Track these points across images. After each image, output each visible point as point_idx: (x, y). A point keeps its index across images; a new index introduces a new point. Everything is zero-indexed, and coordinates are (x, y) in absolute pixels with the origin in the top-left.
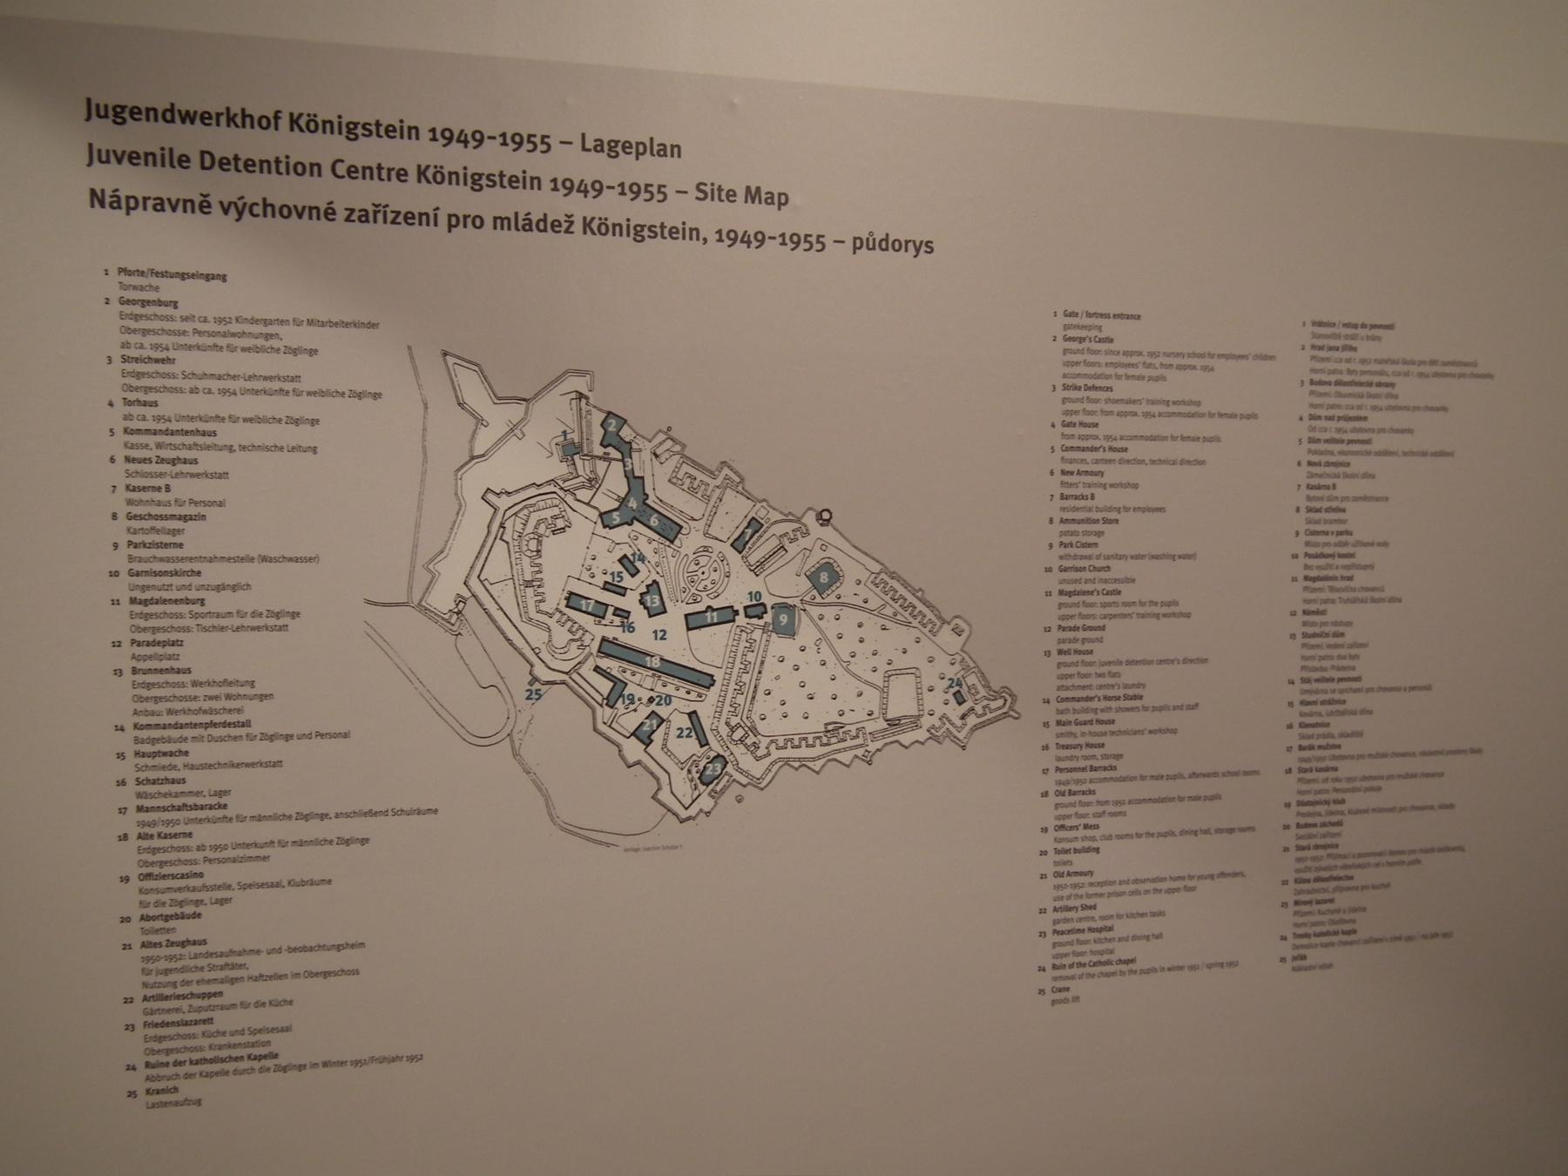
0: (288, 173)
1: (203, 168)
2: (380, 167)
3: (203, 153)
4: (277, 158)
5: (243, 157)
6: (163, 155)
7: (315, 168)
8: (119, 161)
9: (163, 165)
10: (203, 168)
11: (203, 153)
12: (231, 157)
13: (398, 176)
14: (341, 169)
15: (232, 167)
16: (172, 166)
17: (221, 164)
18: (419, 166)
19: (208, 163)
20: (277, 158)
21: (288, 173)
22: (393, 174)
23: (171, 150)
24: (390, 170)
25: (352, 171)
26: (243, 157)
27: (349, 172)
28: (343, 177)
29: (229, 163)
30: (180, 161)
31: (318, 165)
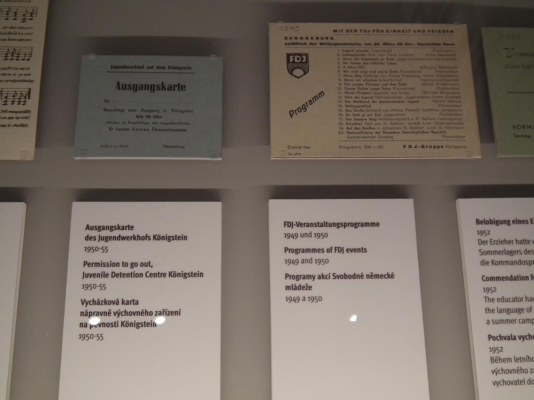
0: (134, 277)
1: (112, 277)
2: (159, 273)
3: (112, 272)
4: (132, 272)
5: (123, 273)
6: (102, 274)
7: (141, 275)
8: (91, 277)
9: (102, 277)
10: (112, 277)
11: (112, 272)
12: (119, 273)
13: (164, 275)
14: (148, 275)
15: (119, 276)
16: (104, 277)
17: (117, 275)
18: (169, 272)
19: (113, 276)
20: (132, 272)
21: (134, 277)
22: (162, 275)
23: (104, 272)
24: (161, 274)
25: (151, 275)
26: (123, 273)
27: (150, 275)
28: (148, 277)
29: (119, 275)
30: (106, 275)
31: (142, 274)
